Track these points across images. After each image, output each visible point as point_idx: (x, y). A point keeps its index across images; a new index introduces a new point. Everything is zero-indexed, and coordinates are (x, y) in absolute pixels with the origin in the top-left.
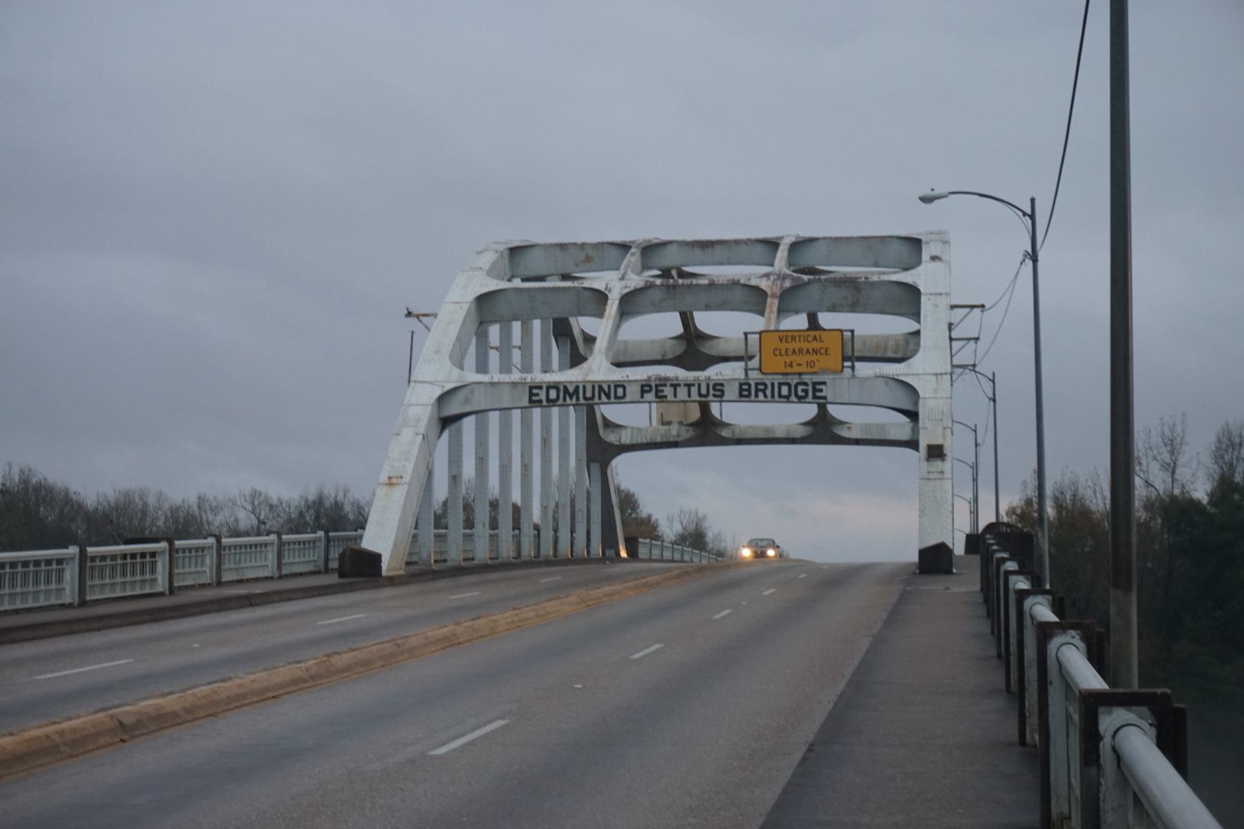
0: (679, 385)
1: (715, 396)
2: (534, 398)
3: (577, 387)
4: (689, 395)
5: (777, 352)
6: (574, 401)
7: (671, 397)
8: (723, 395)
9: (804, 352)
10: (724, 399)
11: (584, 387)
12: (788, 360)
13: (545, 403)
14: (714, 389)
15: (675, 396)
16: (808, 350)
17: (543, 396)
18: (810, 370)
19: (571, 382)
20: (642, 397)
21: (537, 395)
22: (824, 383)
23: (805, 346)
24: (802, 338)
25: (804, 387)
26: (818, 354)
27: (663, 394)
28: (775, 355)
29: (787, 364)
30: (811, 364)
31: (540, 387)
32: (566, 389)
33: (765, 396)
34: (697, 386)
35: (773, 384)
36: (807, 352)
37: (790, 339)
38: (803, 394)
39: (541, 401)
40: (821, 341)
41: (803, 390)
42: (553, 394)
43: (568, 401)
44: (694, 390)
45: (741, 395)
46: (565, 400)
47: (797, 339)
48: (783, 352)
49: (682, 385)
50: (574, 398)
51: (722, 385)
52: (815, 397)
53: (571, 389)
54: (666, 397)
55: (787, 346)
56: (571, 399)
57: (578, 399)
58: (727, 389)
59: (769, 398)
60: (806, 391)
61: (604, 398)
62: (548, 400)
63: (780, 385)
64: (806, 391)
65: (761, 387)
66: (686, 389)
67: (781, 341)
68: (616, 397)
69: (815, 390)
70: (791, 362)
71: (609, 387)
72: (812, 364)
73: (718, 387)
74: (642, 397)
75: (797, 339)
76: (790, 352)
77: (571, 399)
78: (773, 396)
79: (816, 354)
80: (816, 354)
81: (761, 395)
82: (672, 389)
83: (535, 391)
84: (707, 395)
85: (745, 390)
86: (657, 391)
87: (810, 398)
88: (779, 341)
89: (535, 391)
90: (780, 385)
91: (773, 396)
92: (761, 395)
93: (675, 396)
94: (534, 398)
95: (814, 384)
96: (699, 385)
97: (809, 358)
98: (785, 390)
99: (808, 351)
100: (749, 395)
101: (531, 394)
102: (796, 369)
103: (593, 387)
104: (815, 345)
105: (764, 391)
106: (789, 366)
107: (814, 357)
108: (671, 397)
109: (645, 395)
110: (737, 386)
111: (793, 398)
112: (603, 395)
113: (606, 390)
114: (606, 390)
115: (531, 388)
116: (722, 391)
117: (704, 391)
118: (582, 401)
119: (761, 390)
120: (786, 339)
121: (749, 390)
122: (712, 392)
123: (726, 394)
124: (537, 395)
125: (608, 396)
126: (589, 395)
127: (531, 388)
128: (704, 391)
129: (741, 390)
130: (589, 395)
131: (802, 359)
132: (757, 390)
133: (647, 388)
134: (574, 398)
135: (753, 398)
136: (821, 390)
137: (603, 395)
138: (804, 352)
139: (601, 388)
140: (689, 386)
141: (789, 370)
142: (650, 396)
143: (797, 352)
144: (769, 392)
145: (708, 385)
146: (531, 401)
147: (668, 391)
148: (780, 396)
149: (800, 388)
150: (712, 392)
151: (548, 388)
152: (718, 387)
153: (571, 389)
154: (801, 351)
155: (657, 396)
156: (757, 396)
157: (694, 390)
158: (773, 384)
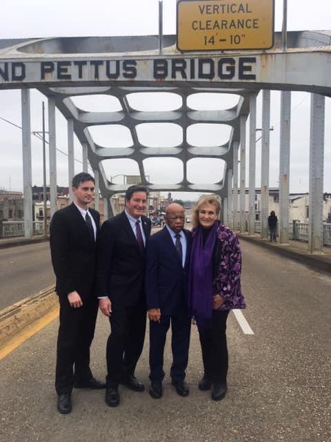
0: (84, 63)
1: (125, 75)
4: (97, 75)
5: (197, 25)
7: (75, 78)
8: (134, 75)
9: (228, 25)
10: (136, 79)
12: (209, 34)
14: (126, 68)
15: (80, 76)
16: (233, 21)
18: (234, 46)
22: (253, 60)
23: (229, 17)
24: (226, 8)
25: (229, 65)
26: (245, 26)
28: (195, 29)
29: (208, 40)
30: (236, 39)
33: (184, 76)
34: (105, 63)
35: (192, 62)
36: (231, 25)
37: (212, 8)
38: (228, 73)
40: (247, 11)
41: (228, 69)
44: (102, 69)
45: (156, 75)
47: (221, 8)
48: (204, 26)
49: (89, 63)
51: (133, 62)
52: (241, 76)
54: (69, 77)
55: (208, 17)
58: (140, 67)
59: (189, 79)
60: (231, 69)
63: (202, 62)
64: (231, 69)
65: (177, 65)
66: (93, 67)
67: (202, 12)
68: (14, 78)
69: (242, 68)
70: (213, 38)
71: (6, 64)
72: (237, 38)
73: (128, 66)
74: (43, 77)
75: (221, 8)
76: (212, 26)
78: (192, 76)
79: (243, 27)
80: (243, 27)
81: (179, 75)
82: (77, 67)
84: (118, 74)
85: (160, 69)
86: (60, 70)
87: (236, 79)
88: (199, 12)
90: (202, 62)
91: (192, 76)
92: (179, 75)
93: (80, 76)
95: (242, 60)
96: (108, 62)
97: (234, 31)
98: (206, 69)
99: (233, 24)
100: (166, 74)
102: (218, 45)
104: (242, 16)
105: (182, 70)
106: (210, 42)
107: (240, 31)
110: (151, 64)
111: (216, 79)
116: (134, 70)
117: (113, 71)
119: (179, 69)
120: (207, 9)
121: (165, 69)
122: (122, 71)
123: (138, 72)
128: (113, 71)
129: (156, 69)
131: (226, 33)
132: (175, 69)
133: (49, 67)
135: (169, 78)
136: (249, 69)
138: (228, 25)
140: (97, 63)
141: (210, 46)
142: (52, 77)
143: (220, 25)
145: (118, 62)
147: (73, 71)
148: (201, 75)
149: (225, 66)
150: (122, 71)
154: (224, 23)
155: (59, 76)
156: (174, 76)
157: (102, 69)
158: (192, 62)
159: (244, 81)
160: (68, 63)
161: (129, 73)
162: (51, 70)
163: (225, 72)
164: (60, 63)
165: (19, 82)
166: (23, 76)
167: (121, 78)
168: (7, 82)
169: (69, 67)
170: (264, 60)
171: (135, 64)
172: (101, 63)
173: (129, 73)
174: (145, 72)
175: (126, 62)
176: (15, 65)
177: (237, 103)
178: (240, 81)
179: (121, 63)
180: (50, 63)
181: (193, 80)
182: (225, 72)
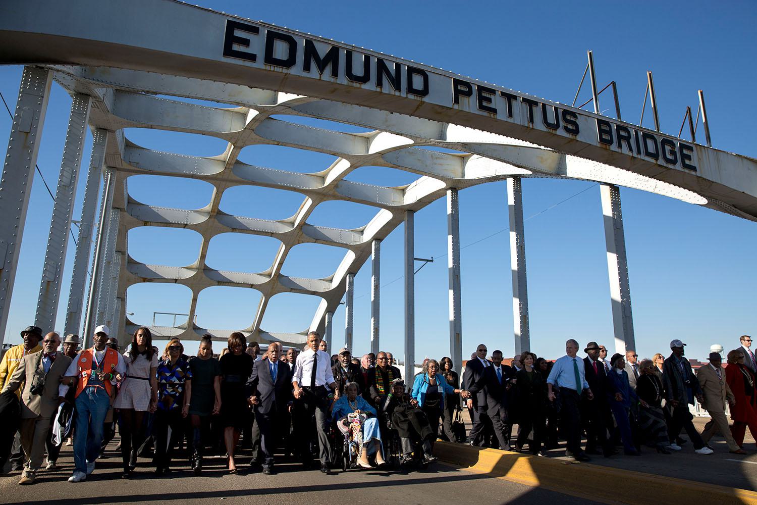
0: (515, 98)
1: (566, 129)
2: (236, 47)
3: (335, 51)
4: (531, 120)
6: (327, 75)
10: (579, 138)
11: (349, 55)
13: (260, 64)
17: (257, 45)
19: (325, 41)
20: (457, 101)
21: (246, 42)
27: (489, 105)
31: (254, 30)
32: (310, 46)
39: (252, 57)
42: (281, 50)
43: (314, 72)
44: (538, 112)
46: (307, 68)
50: (328, 70)
51: (574, 114)
53: (323, 50)
54: (494, 111)
56: (321, 69)
57: (335, 73)
60: (673, 152)
61: (387, 88)
62: (269, 58)
64: (673, 152)
71: (398, 66)
73: (568, 117)
74: (457, 101)
77: (321, 69)
81: (624, 144)
83: (238, 33)
84: (557, 126)
86: (481, 99)
89: (238, 33)
91: (639, 152)
92: (624, 144)
93: (511, 115)
94: (236, 47)
101: (230, 39)
103: (367, 58)
105: (628, 139)
108: (502, 115)
109: (461, 98)
112: (385, 81)
113: (393, 73)
114: (393, 73)
115: (232, 25)
118: (343, 79)
121: (609, 132)
122: (562, 123)
124: (246, 42)
125: (397, 84)
126: (358, 70)
127: (232, 25)
130: (358, 70)
132: (620, 138)
134: (328, 70)
135: (614, 147)
137: (385, 81)
139: (381, 64)
140: (531, 103)
142: (470, 104)
144: (633, 141)
146: (228, 52)
147: (498, 103)
149: (668, 148)
150: (562, 123)
151: (273, 36)
152: (568, 117)
153: (323, 50)
155: (481, 107)
157: (538, 112)
159: (686, 171)
160: (493, 92)
161: (570, 127)
162: (469, 94)
163: (669, 156)
164: (481, 89)
165: (419, 99)
166: (425, 92)
167: (561, 132)
168: (397, 93)
169: (492, 97)
170: (699, 152)
171: (576, 117)
172: (536, 103)
173: (570, 127)
174: (590, 133)
175: (566, 112)
176: (412, 71)
177: (354, 279)
178: (683, 170)
179: (560, 111)
180: (467, 84)
181: (639, 156)
182: (669, 156)
